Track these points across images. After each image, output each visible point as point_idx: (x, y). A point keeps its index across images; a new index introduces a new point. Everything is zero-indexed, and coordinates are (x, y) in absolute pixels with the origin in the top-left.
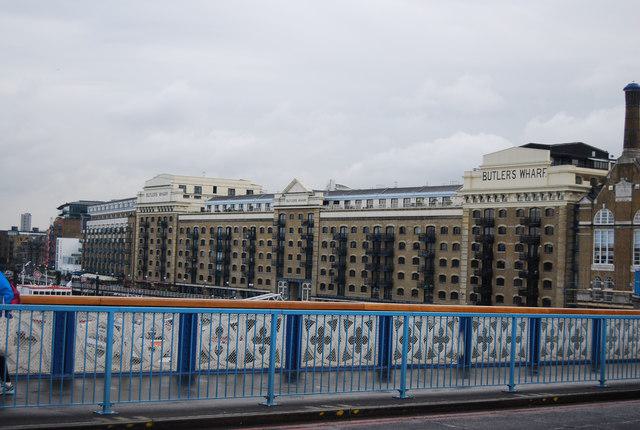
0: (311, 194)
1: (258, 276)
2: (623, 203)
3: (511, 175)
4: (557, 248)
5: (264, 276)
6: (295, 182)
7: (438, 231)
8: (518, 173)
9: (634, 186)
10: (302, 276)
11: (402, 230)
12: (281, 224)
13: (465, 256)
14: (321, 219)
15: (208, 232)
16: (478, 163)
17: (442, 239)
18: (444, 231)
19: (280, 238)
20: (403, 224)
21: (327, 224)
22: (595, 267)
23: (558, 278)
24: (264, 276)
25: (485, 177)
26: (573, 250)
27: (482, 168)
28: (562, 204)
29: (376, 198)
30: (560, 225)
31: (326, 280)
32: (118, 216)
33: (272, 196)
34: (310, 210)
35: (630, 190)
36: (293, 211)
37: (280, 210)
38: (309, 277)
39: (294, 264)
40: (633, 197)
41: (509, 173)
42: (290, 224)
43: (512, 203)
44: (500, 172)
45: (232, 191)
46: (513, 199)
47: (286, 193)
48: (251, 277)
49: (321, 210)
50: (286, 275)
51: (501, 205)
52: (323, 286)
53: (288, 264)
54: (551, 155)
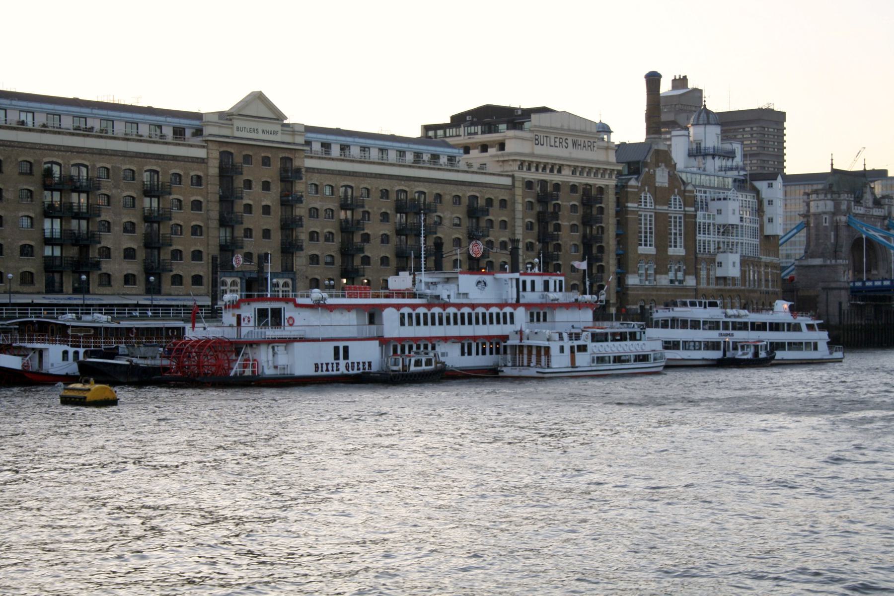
0: (291, 129)
2: (661, 187)
3: (564, 144)
4: (608, 230)
11: (439, 196)
12: (227, 171)
14: (308, 170)
20: (438, 189)
21: (316, 179)
22: (642, 250)
29: (356, 145)
35: (667, 176)
40: (669, 184)
43: (566, 177)
44: (552, 137)
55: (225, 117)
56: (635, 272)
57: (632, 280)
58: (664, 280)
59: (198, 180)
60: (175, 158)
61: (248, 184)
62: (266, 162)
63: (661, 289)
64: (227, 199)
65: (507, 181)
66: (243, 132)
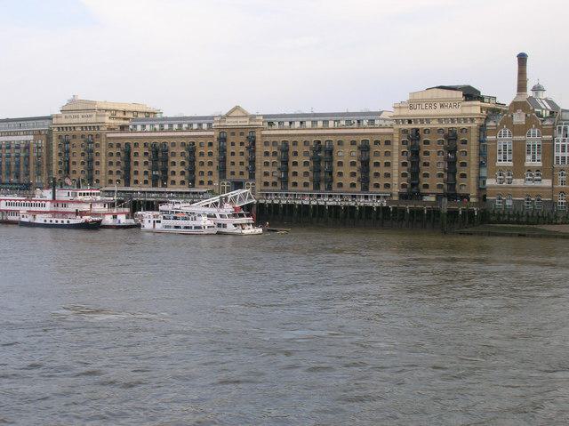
0: (252, 117)
6: (237, 108)
7: (371, 143)
8: (438, 105)
9: (526, 116)
10: (246, 176)
12: (222, 139)
13: (396, 160)
14: (263, 136)
15: (141, 146)
16: (406, 98)
17: (374, 149)
18: (377, 142)
19: (222, 151)
20: (341, 138)
22: (498, 164)
23: (472, 172)
25: (411, 107)
26: (482, 153)
27: (409, 101)
28: (474, 125)
30: (473, 138)
32: (27, 133)
33: (213, 118)
34: (253, 129)
36: (234, 131)
37: (222, 130)
38: (252, 176)
41: (431, 103)
42: (231, 139)
43: (435, 124)
46: (435, 122)
47: (227, 116)
49: (263, 129)
50: (229, 176)
51: (425, 126)
52: (266, 184)
54: (464, 95)
55: (223, 118)
56: (492, 178)
57: (490, 182)
58: (518, 182)
59: (211, 144)
60: (200, 136)
61: (233, 144)
62: (242, 134)
63: (517, 188)
64: (222, 151)
65: (391, 131)
66: (230, 123)
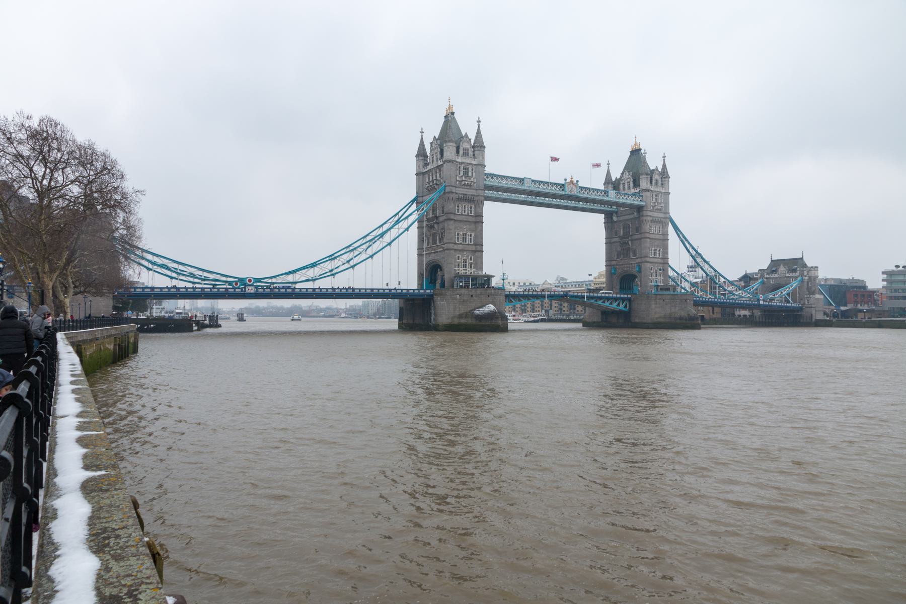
1: (536, 309)
5: (537, 309)
10: (549, 308)
24: (537, 309)
25: (599, 278)
31: (556, 309)
33: (539, 285)
38: (551, 309)
39: (546, 305)
45: (530, 284)
47: (544, 284)
48: (533, 309)
50: (545, 309)
53: (545, 305)
